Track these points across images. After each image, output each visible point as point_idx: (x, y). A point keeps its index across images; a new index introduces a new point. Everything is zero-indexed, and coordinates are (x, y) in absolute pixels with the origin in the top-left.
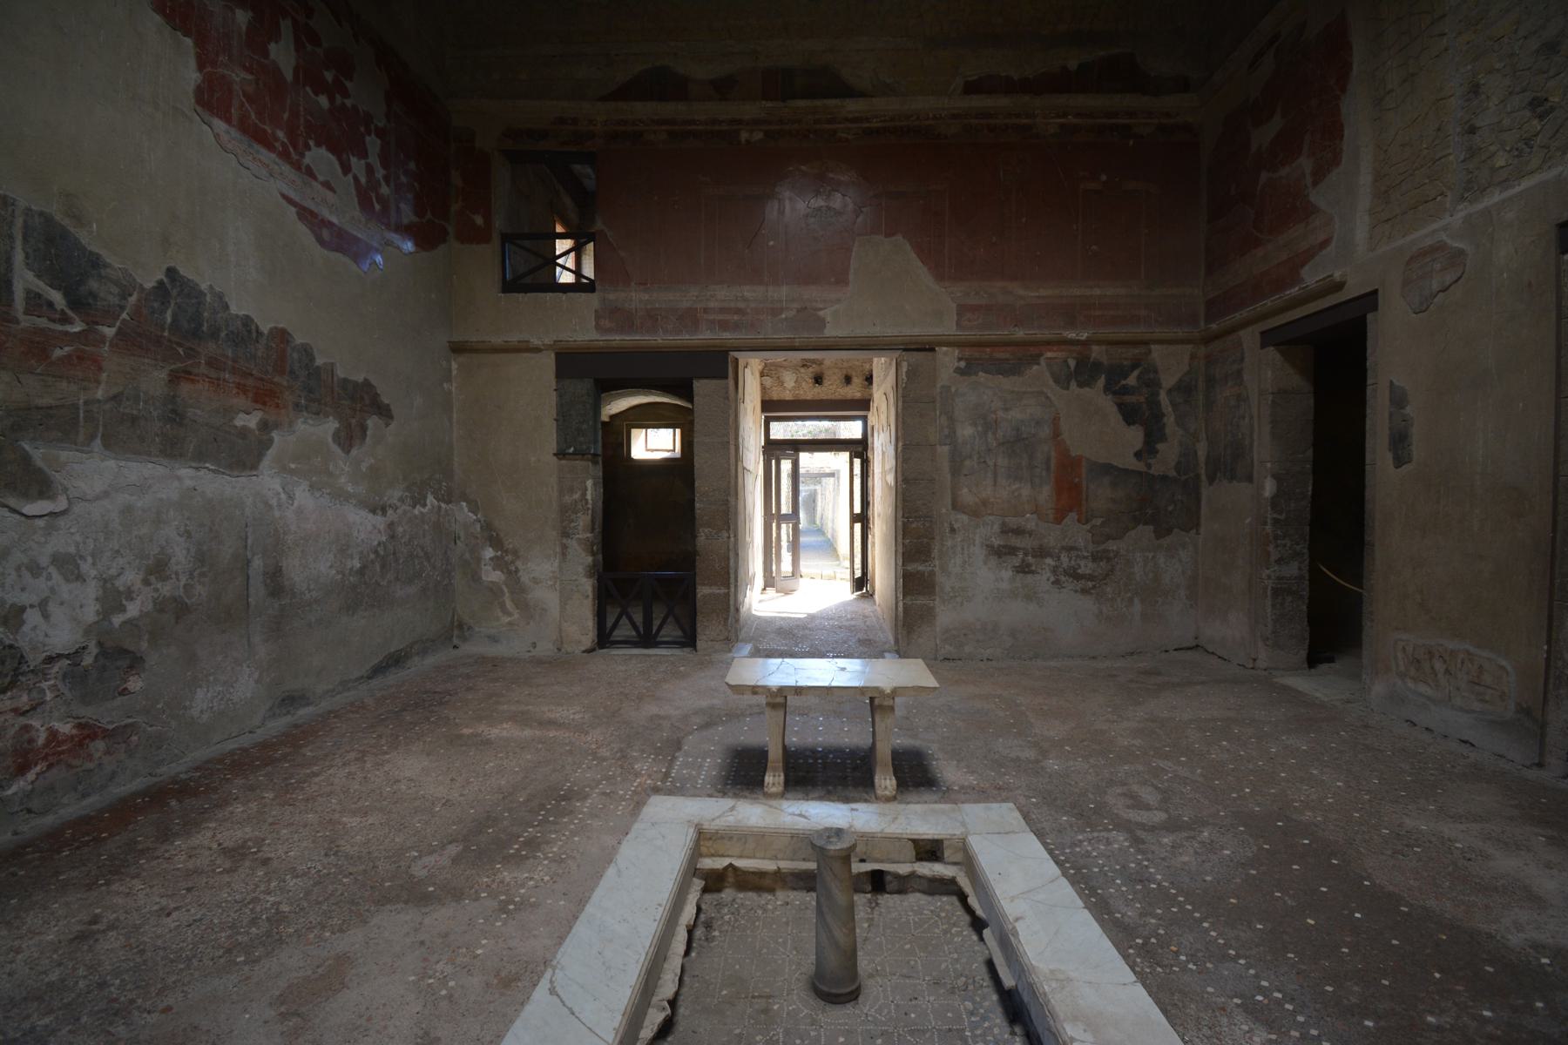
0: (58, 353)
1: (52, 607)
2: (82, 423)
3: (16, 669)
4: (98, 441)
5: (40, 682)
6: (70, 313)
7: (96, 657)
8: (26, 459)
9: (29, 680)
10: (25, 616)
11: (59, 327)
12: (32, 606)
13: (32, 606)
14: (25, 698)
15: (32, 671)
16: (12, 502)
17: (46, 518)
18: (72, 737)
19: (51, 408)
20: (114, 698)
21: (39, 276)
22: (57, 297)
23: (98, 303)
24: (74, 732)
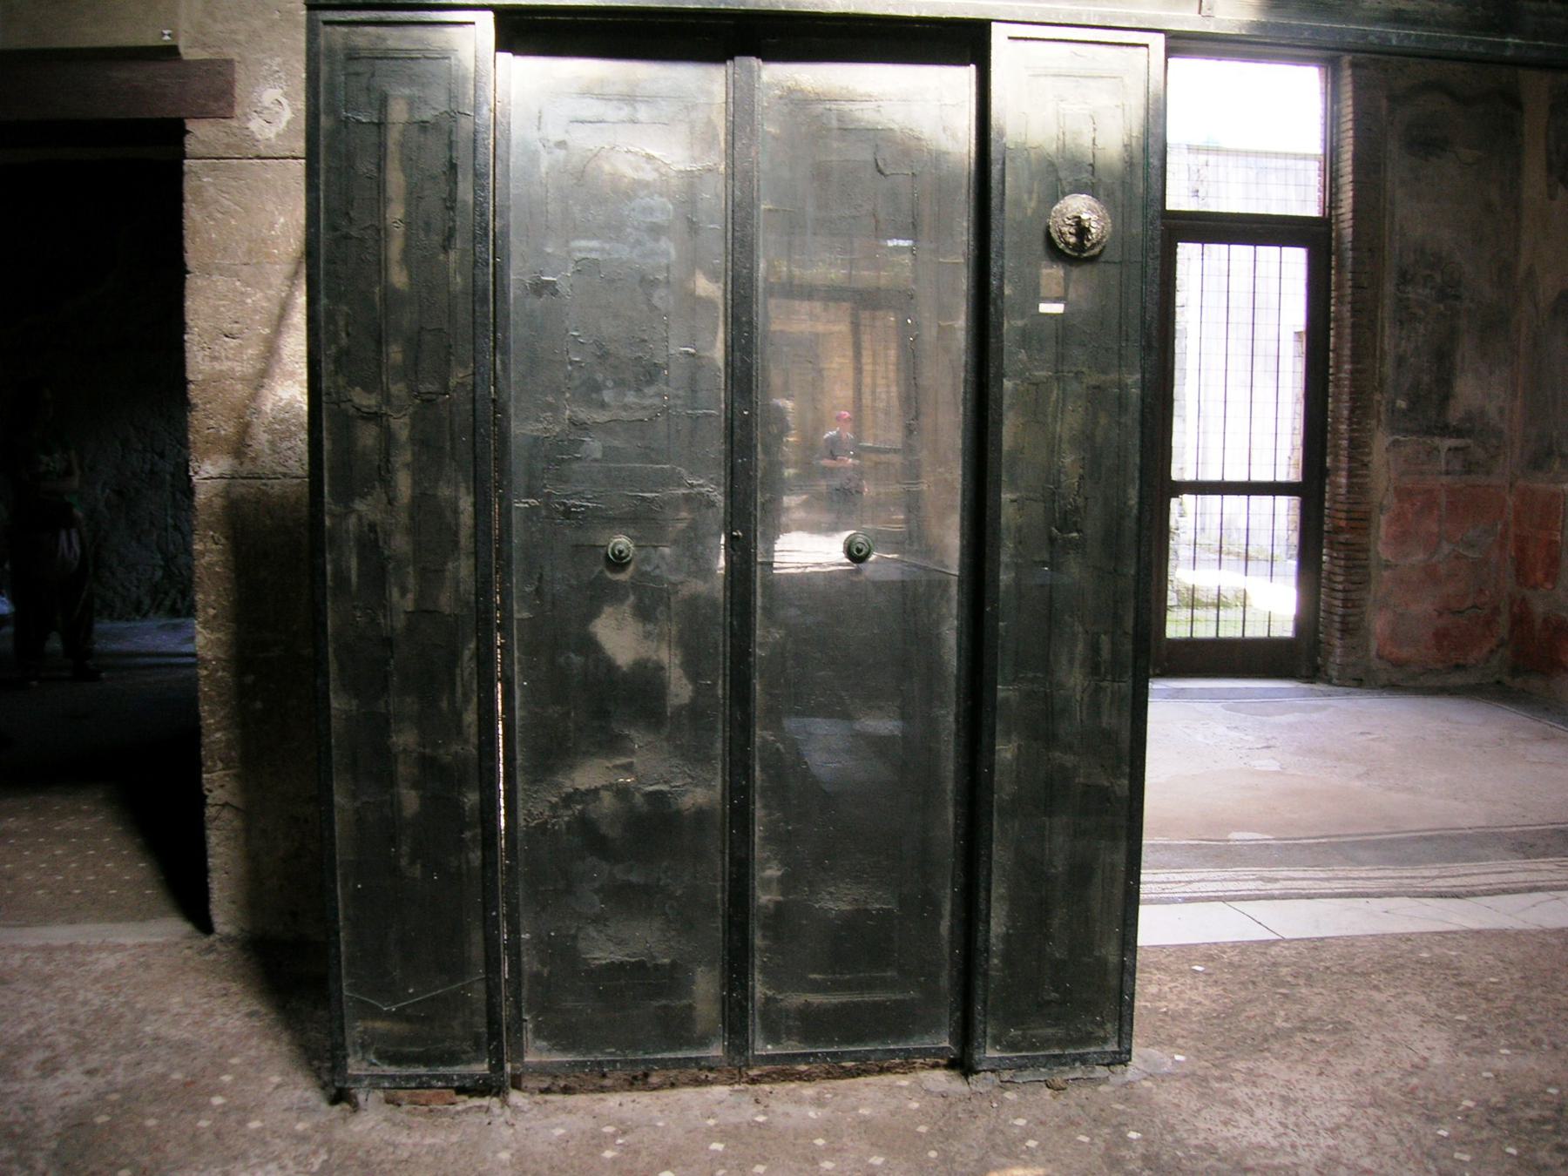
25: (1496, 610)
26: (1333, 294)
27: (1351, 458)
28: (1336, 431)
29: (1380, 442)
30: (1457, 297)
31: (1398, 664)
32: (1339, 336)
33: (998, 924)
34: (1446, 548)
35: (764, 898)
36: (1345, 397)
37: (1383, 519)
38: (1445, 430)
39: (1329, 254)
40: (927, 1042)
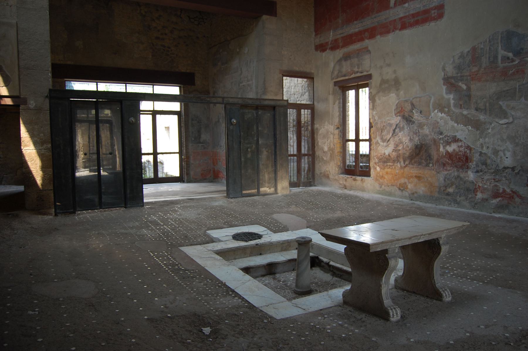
0: (511, 72)
1: (506, 152)
2: (517, 93)
3: (495, 168)
4: (523, 98)
5: (501, 174)
6: (515, 58)
7: (520, 170)
8: (501, 107)
9: (499, 172)
10: (499, 153)
11: (511, 64)
12: (501, 151)
13: (501, 151)
14: (497, 177)
15: (500, 170)
16: (497, 120)
17: (506, 124)
18: (510, 194)
19: (508, 90)
20: (525, 187)
21: (505, 51)
22: (510, 55)
23: (524, 51)
24: (511, 192)
25: (210, 170)
26: (182, 122)
27: (186, 148)
28: (183, 144)
29: (190, 145)
30: (201, 122)
31: (196, 179)
32: (183, 129)
33: (128, 191)
34: (202, 161)
35: (103, 190)
36: (184, 138)
37: (191, 157)
38: (200, 143)
39: (181, 116)
40: (122, 206)
